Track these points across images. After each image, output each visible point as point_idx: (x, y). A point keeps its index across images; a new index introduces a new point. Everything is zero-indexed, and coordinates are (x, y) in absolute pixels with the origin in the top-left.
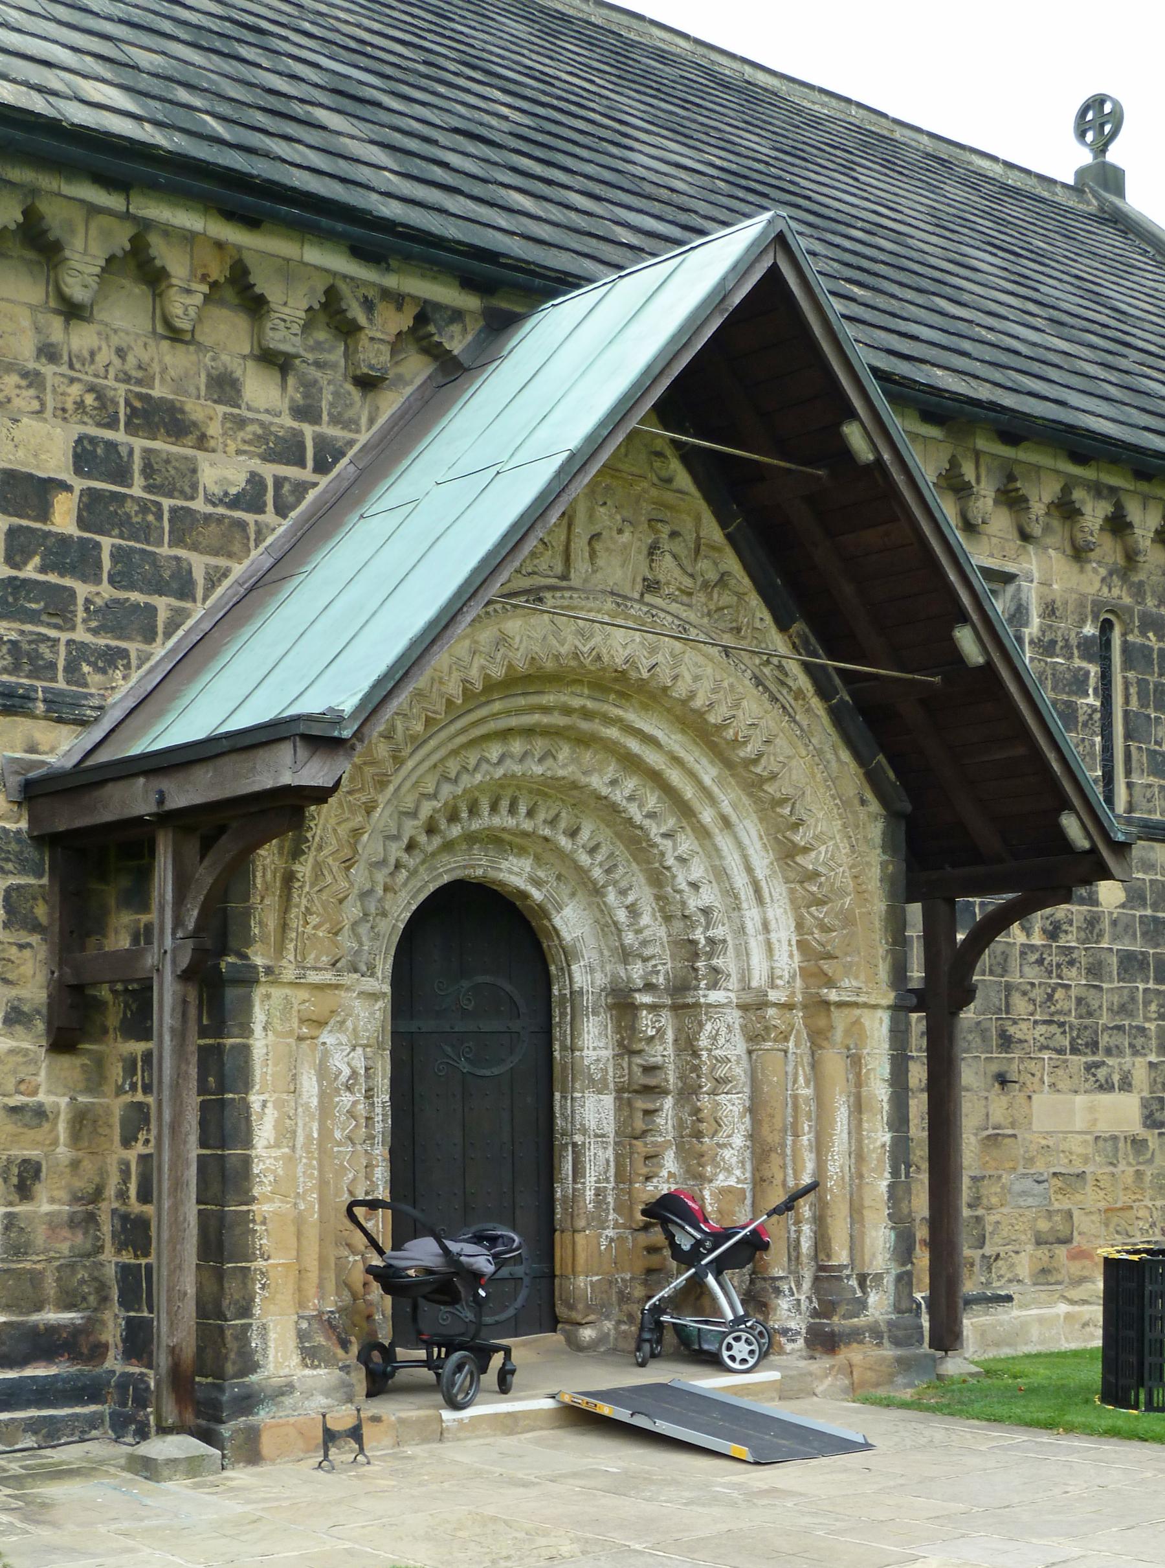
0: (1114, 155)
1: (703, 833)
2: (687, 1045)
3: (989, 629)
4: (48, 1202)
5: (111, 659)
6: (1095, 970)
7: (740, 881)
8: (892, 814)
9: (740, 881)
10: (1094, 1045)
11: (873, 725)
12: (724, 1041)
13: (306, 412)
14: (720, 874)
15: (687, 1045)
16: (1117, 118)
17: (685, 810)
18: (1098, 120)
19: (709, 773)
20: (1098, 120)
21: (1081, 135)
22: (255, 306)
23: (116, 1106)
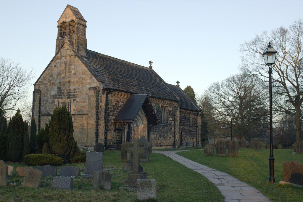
0: (152, 65)
1: (139, 121)
2: (137, 132)
3: (154, 113)
4: (114, 139)
7: (140, 124)
8: (147, 120)
9: (140, 124)
11: (146, 116)
12: (139, 132)
13: (123, 100)
14: (139, 123)
15: (137, 132)
16: (152, 63)
17: (138, 120)
18: (151, 63)
19: (140, 118)
20: (151, 63)
21: (149, 63)
23: (116, 135)
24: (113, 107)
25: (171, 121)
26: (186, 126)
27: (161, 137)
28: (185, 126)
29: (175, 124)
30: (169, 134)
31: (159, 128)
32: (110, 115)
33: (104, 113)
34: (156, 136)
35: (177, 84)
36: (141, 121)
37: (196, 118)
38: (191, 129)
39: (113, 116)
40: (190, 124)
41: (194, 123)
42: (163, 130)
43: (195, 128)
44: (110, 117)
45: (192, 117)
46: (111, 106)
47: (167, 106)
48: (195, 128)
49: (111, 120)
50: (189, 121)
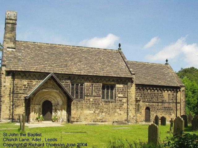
5: (28, 92)
6: (90, 104)
10: (89, 108)
22: (36, 76)
24: (24, 87)
25: (121, 97)
26: (155, 102)
27: (104, 114)
28: (153, 102)
29: (128, 101)
30: (118, 110)
31: (100, 104)
32: (18, 94)
33: (9, 92)
34: (94, 112)
35: (166, 62)
36: (60, 97)
37: (175, 94)
38: (166, 105)
39: (24, 94)
40: (162, 101)
41: (172, 99)
42: (106, 106)
43: (175, 104)
44: (20, 95)
45: (166, 94)
46: (21, 86)
47: (113, 83)
48: (175, 104)
49: (20, 97)
50: (161, 97)
